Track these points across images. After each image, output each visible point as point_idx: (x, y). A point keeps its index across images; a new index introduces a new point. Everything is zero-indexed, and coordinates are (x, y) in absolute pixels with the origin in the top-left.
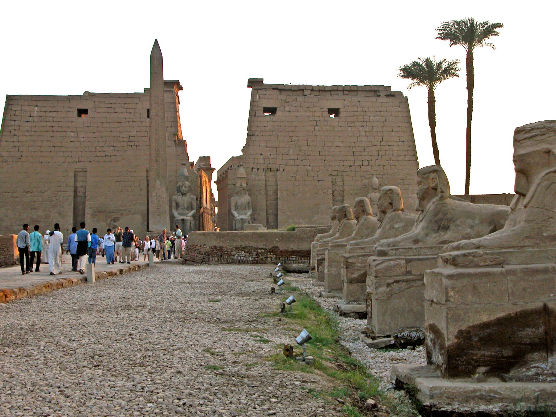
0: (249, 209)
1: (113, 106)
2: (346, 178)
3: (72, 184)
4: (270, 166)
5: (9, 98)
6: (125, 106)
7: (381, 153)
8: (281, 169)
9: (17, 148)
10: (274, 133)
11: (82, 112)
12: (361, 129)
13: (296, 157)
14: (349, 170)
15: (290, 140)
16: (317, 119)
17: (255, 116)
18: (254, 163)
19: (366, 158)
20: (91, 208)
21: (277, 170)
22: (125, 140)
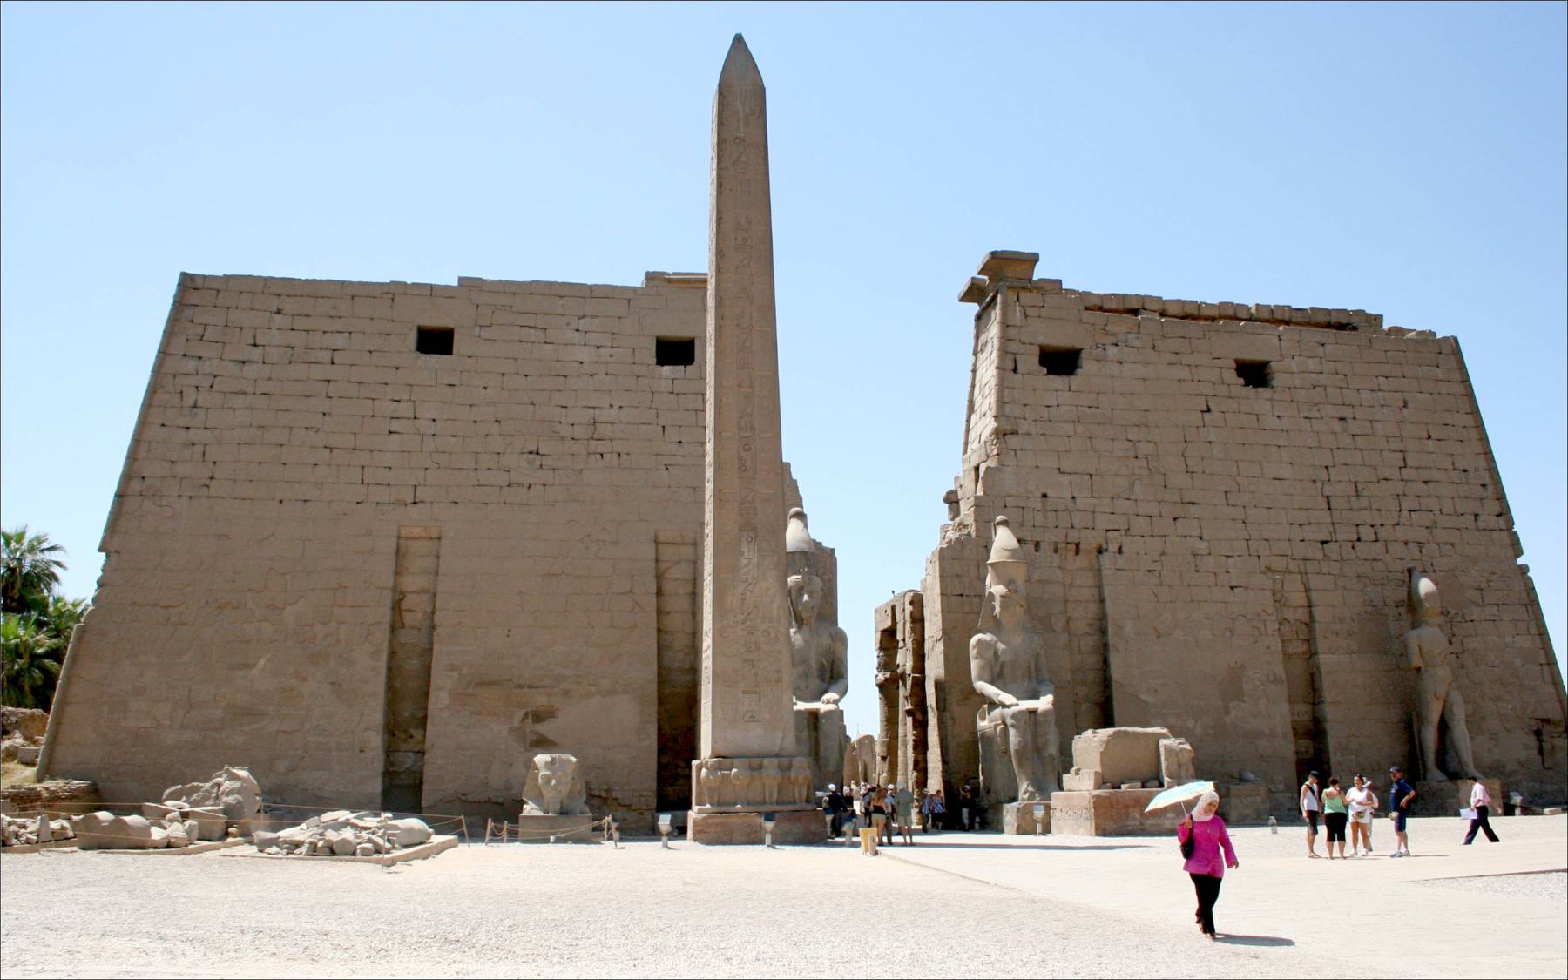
1: (541, 321)
2: (1315, 582)
3: (388, 580)
4: (1074, 536)
5: (188, 283)
6: (582, 324)
7: (1407, 504)
8: (1113, 548)
9: (198, 449)
10: (1080, 429)
11: (435, 341)
12: (1337, 426)
13: (1153, 509)
14: (1320, 556)
16: (1207, 389)
17: (1015, 370)
18: (1022, 525)
19: (1367, 517)
20: (452, 668)
21: (1100, 551)
22: (579, 432)
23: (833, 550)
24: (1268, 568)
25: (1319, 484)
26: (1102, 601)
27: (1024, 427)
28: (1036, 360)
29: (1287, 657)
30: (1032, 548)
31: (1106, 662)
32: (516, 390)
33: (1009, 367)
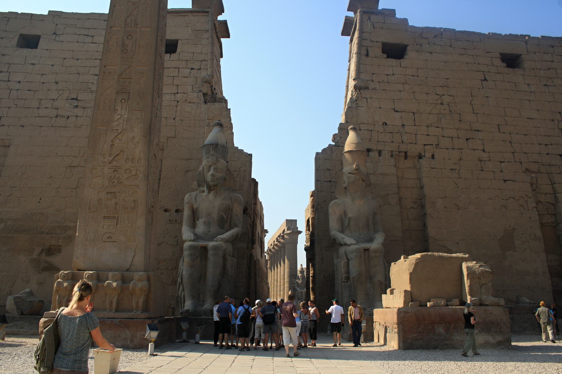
0: (376, 232)
1: (91, 32)
4: (403, 148)
8: (428, 155)
15: (439, 102)
17: (367, 55)
18: (370, 140)
21: (420, 157)
23: (251, 155)
24: (527, 170)
25: (556, 122)
26: (422, 187)
27: (372, 85)
28: (380, 50)
29: (542, 225)
30: (377, 154)
31: (425, 225)
32: (71, 66)
33: (363, 53)
